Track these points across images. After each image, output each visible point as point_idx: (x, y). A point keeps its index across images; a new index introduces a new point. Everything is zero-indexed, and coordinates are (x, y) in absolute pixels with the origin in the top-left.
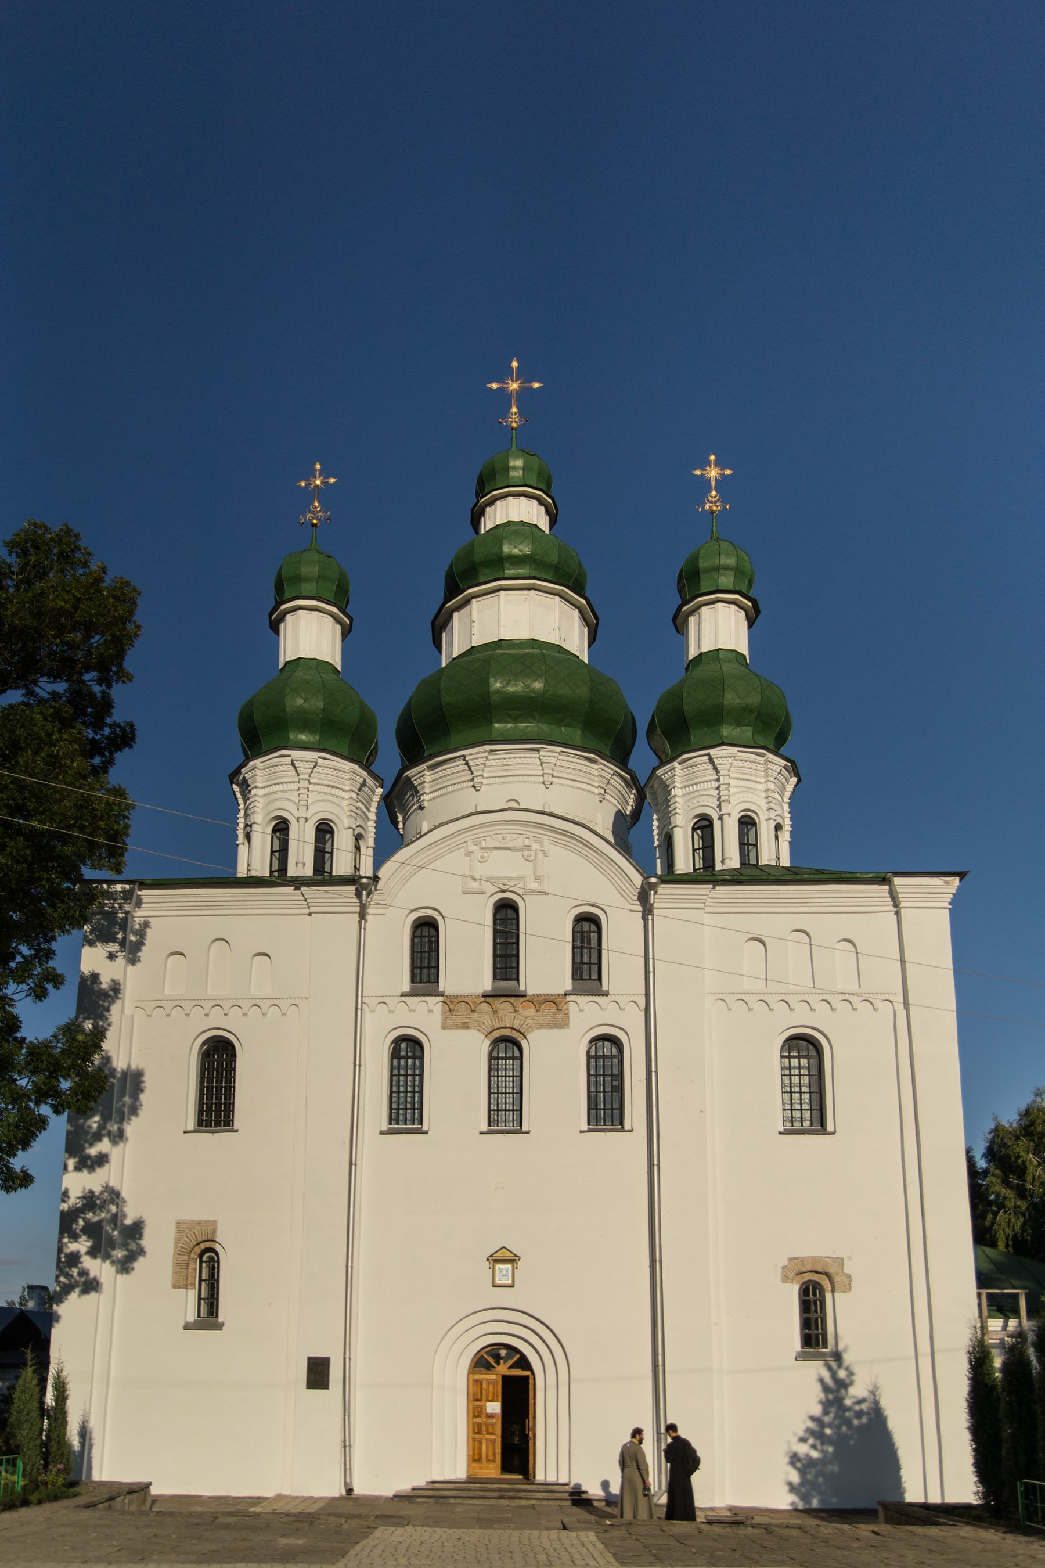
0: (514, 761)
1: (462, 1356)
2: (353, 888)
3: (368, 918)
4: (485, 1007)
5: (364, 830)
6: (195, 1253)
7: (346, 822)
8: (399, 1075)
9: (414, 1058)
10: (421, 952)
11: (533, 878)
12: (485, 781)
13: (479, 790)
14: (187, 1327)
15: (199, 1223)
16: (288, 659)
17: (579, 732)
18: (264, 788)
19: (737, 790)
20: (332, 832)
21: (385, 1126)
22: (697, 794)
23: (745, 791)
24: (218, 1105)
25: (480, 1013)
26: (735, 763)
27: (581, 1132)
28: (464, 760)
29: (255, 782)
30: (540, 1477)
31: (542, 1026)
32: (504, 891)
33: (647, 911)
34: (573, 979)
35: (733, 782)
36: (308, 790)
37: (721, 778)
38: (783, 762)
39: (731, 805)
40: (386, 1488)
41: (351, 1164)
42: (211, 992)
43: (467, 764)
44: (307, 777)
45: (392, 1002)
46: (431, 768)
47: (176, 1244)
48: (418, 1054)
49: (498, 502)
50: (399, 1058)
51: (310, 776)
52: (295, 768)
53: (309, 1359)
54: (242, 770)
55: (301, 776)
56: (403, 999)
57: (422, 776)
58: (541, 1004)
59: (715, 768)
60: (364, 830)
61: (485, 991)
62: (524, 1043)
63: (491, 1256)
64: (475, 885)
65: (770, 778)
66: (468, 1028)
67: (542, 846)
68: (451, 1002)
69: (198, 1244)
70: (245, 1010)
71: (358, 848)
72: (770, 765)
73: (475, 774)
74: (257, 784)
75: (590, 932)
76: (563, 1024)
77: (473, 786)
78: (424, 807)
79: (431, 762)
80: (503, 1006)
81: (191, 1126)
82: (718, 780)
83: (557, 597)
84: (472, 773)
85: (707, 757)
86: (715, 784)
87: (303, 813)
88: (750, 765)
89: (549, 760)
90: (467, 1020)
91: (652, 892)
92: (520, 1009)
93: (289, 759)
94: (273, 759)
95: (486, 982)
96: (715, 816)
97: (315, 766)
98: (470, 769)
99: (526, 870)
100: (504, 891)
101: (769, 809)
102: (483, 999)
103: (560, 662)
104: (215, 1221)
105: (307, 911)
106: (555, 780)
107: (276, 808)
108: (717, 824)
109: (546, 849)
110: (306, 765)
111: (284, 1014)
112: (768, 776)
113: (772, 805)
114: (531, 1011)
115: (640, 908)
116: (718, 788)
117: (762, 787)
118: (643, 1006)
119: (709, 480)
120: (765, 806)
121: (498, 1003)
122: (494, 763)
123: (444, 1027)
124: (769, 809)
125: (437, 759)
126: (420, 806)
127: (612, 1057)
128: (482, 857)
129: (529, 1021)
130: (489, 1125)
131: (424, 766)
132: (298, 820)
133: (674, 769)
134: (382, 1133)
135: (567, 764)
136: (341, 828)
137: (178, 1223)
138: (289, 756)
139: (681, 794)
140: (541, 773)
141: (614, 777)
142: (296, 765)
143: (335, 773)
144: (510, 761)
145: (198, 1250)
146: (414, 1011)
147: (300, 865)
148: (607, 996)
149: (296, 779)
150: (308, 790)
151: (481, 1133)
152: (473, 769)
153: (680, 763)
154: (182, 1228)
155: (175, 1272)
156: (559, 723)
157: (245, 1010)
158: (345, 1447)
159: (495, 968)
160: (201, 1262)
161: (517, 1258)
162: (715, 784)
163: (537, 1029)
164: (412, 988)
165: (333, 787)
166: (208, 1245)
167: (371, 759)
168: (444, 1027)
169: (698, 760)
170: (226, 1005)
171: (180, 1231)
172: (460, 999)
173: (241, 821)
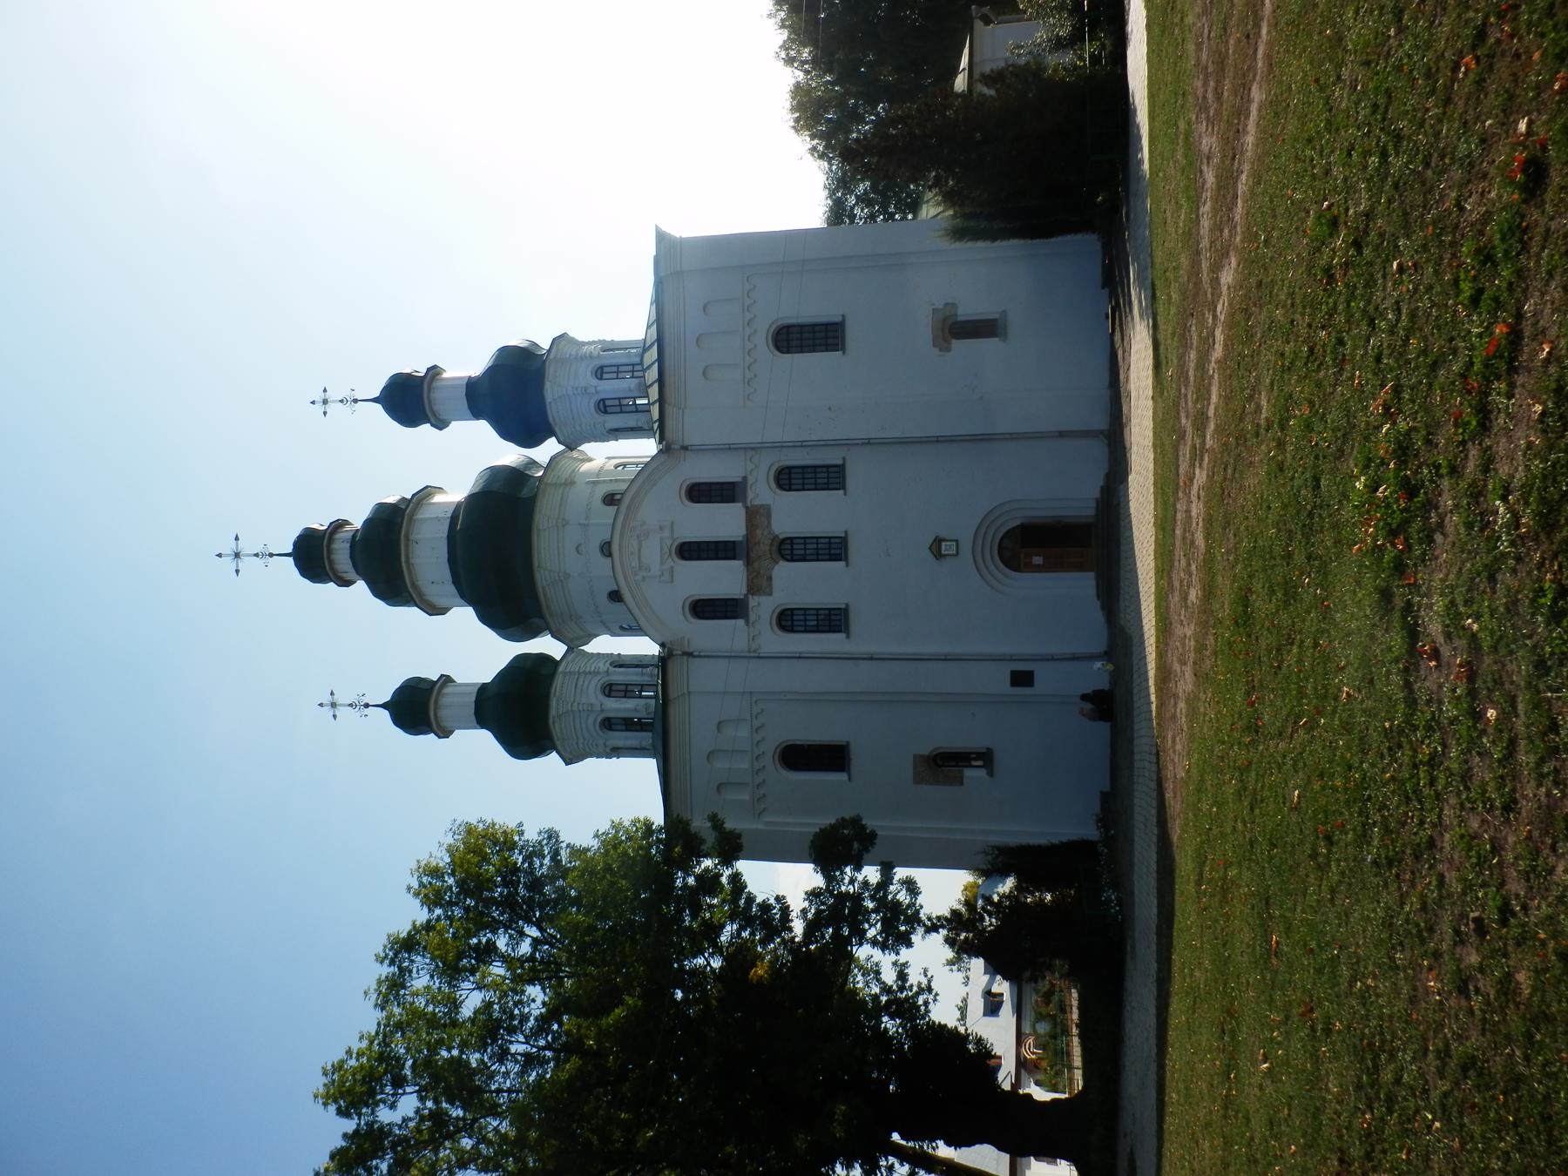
3: (691, 650)
4: (756, 565)
9: (792, 615)
14: (991, 774)
15: (915, 768)
20: (611, 685)
31: (769, 523)
41: (872, 659)
42: (745, 765)
48: (789, 612)
50: (792, 626)
62: (781, 537)
95: (737, 566)
100: (670, 554)
114: (759, 532)
123: (771, 594)
129: (765, 533)
154: (918, 779)
168: (771, 594)
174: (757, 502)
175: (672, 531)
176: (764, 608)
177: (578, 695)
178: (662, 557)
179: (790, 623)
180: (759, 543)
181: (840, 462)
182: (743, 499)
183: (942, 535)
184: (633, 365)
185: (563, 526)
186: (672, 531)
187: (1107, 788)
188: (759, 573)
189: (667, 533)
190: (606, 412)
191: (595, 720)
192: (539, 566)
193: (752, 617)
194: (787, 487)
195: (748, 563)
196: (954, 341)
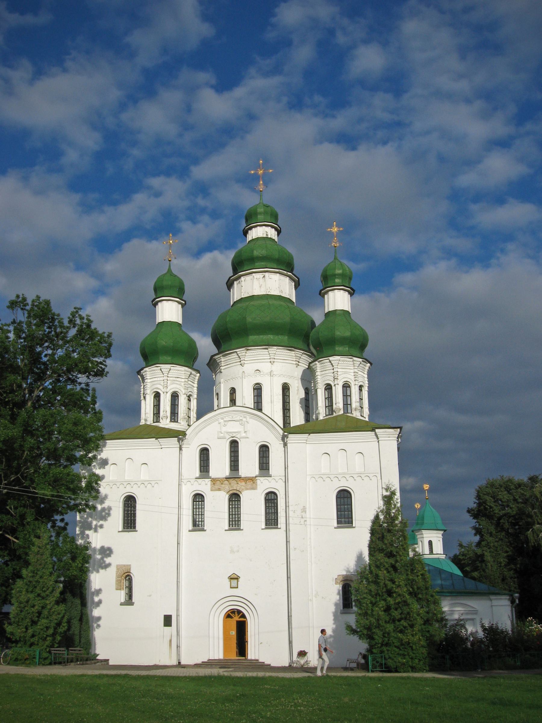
0: (258, 353)
1: (221, 614)
2: (177, 439)
3: (183, 449)
4: (226, 482)
5: (192, 392)
6: (123, 577)
7: (184, 391)
8: (196, 508)
10: (203, 460)
11: (243, 432)
12: (246, 362)
13: (243, 366)
15: (124, 566)
16: (159, 322)
17: (286, 337)
18: (150, 379)
19: (341, 373)
20: (178, 396)
21: (191, 529)
22: (325, 375)
23: (345, 374)
24: (131, 520)
25: (224, 485)
26: (340, 362)
27: (262, 529)
28: (237, 353)
29: (146, 377)
30: (249, 658)
31: (247, 489)
32: (233, 437)
33: (285, 445)
34: (260, 469)
35: (339, 370)
36: (167, 380)
37: (334, 369)
38: (361, 360)
39: (339, 380)
40: (192, 662)
41: (178, 543)
42: (126, 478)
43: (238, 355)
44: (167, 375)
45: (192, 481)
46: (224, 356)
47: (117, 574)
49: (253, 229)
51: (168, 374)
52: (162, 372)
53: (165, 616)
54: (142, 371)
55: (165, 375)
56: (196, 480)
57: (220, 359)
58: (246, 481)
59: (332, 364)
60: (192, 392)
61: (227, 476)
62: (241, 495)
63: (229, 577)
64: (222, 435)
65: (355, 367)
66: (220, 490)
67: (246, 419)
68: (214, 481)
69: (124, 573)
70: (139, 485)
71: (189, 400)
72: (355, 362)
73: (241, 359)
74: (147, 378)
75: (266, 451)
76: (254, 488)
77: (241, 364)
78: (222, 372)
79: (223, 354)
80: (233, 482)
81: (121, 529)
82: (333, 369)
83: (278, 274)
84: (240, 359)
85: (328, 360)
86: (332, 371)
87: (165, 390)
88: (346, 362)
89: (272, 352)
90: (220, 487)
91: (286, 438)
92: (239, 483)
93: (159, 368)
94: (153, 368)
96: (333, 385)
97: (170, 370)
98: (239, 357)
99: (240, 429)
100: (233, 437)
101: (355, 380)
102: (225, 479)
103: (277, 308)
104: (130, 565)
105: (160, 447)
106: (275, 360)
107: (155, 388)
108: (333, 388)
109: (248, 420)
110: (166, 370)
111: (153, 487)
112: (355, 366)
113: (356, 379)
114: (243, 483)
115: (283, 443)
116: (334, 372)
117: (352, 371)
118: (284, 481)
119: (333, 233)
120: (353, 379)
121: (231, 480)
122: (249, 354)
123: (211, 490)
124: (355, 380)
125: (226, 353)
126: (220, 371)
127: (274, 499)
128: (224, 424)
130: (229, 527)
131: (221, 355)
132: (164, 393)
133: (316, 364)
134: (190, 531)
135: (281, 353)
136: (182, 394)
137: (117, 566)
138: (159, 366)
139: (320, 375)
140: (269, 358)
141: (303, 355)
142: (162, 370)
143: (178, 372)
144: (256, 354)
145: (124, 576)
146: (200, 484)
147: (165, 412)
148: (271, 477)
149: (163, 375)
150: (167, 380)
151: (225, 530)
152: (240, 357)
153: (318, 362)
155: (116, 586)
156: (277, 334)
157: (139, 485)
158: (178, 647)
159: (231, 466)
160: (126, 580)
161: (239, 577)
162: (332, 371)
163: (246, 490)
164: (200, 475)
165: (178, 378)
166: (128, 574)
167: (195, 360)
168: (211, 490)
169: (326, 361)
170: (132, 484)
171: (117, 569)
172: (217, 479)
173: (142, 392)
174: (258, 482)
175: (243, 438)
176: (204, 486)
177: (171, 379)
178: (231, 432)
179: (197, 500)
180: (238, 483)
181: (279, 526)
182: (261, 475)
183: (240, 580)
184: (351, 404)
185: (270, 362)
186: (243, 438)
187: (111, 663)
188: (222, 484)
189: (244, 435)
190: (325, 389)
191: (159, 389)
192: (248, 350)
193: (200, 480)
194: (267, 498)
195: (227, 478)
196: (341, 586)
